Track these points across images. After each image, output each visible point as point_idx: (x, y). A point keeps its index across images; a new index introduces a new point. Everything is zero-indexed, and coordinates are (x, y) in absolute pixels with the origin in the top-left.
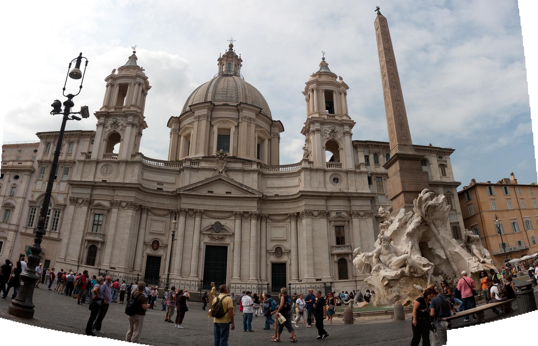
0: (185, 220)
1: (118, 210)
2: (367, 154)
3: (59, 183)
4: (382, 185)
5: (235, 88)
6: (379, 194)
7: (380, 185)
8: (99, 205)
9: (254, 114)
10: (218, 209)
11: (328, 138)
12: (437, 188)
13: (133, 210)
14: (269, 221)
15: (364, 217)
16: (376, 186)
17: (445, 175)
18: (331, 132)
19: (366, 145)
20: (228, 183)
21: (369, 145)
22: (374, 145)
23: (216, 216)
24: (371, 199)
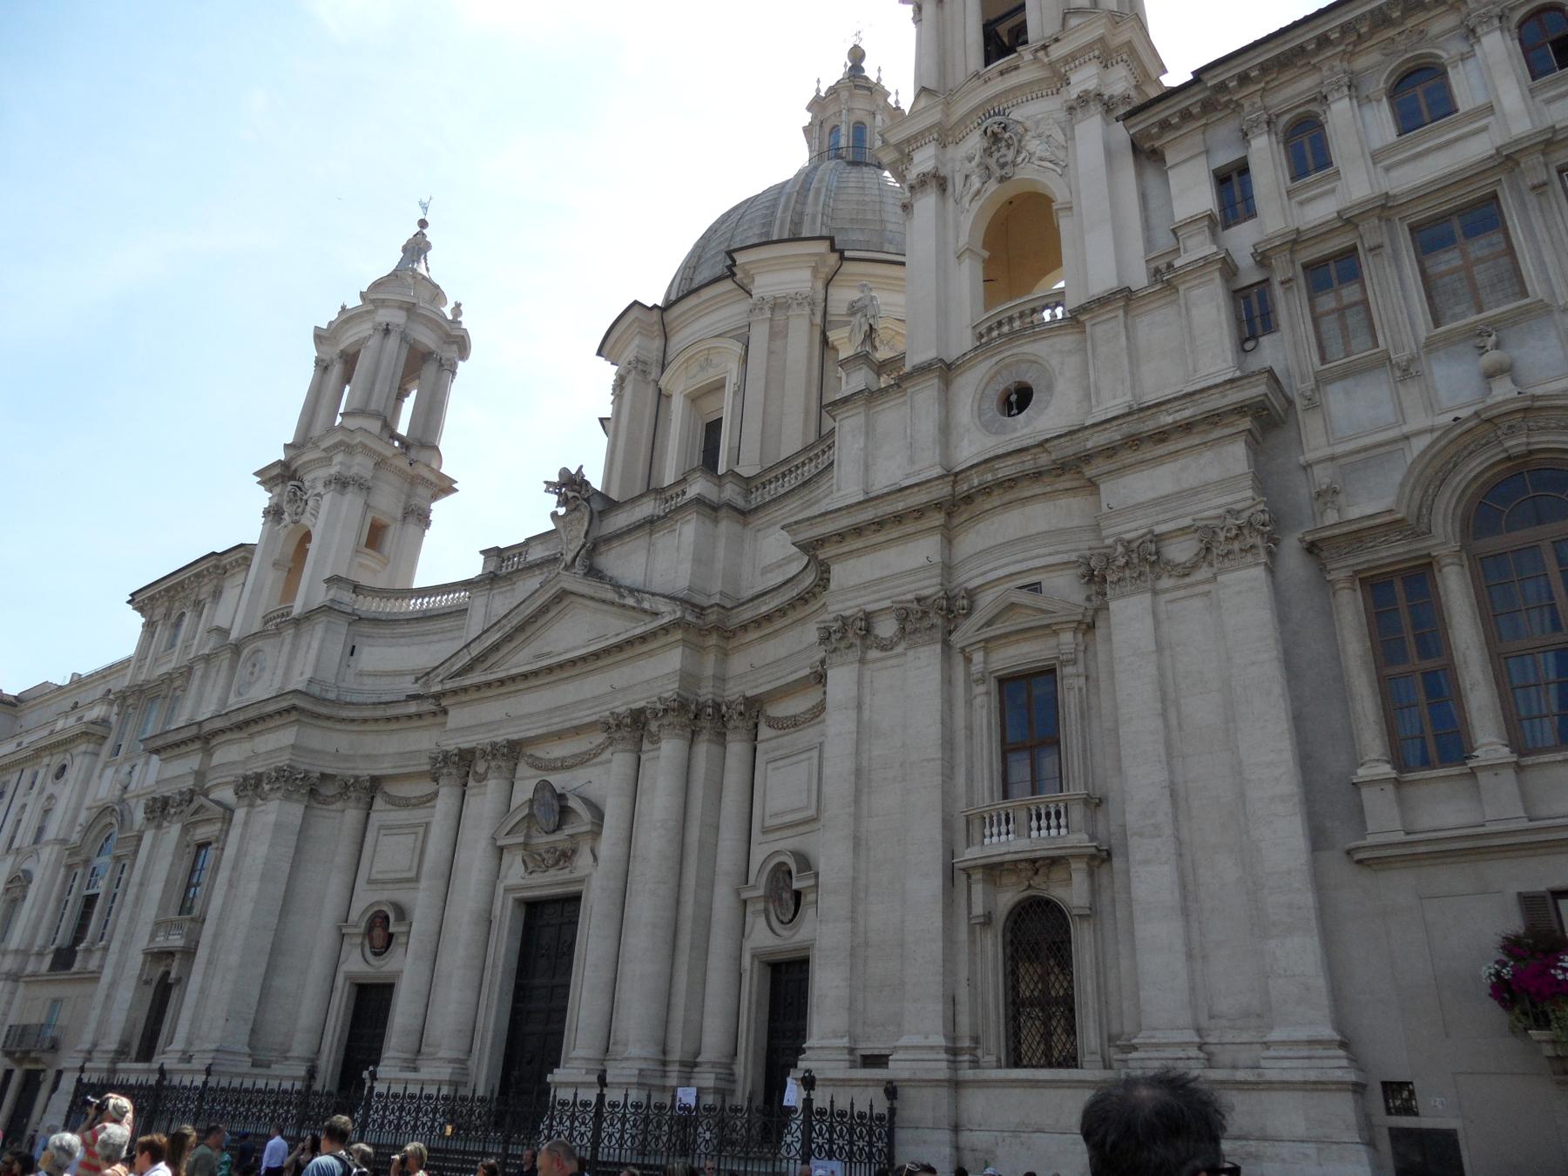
0: (458, 804)
1: (248, 813)
3: (147, 763)
4: (1365, 302)
5: (768, 208)
6: (1322, 381)
7: (1341, 311)
9: (807, 274)
10: (557, 723)
11: (978, 192)
13: (288, 797)
14: (765, 732)
15: (1203, 573)
18: (988, 152)
19: (1208, 106)
20: (592, 598)
21: (1222, 87)
22: (1264, 68)
23: (556, 759)
24: (1246, 423)
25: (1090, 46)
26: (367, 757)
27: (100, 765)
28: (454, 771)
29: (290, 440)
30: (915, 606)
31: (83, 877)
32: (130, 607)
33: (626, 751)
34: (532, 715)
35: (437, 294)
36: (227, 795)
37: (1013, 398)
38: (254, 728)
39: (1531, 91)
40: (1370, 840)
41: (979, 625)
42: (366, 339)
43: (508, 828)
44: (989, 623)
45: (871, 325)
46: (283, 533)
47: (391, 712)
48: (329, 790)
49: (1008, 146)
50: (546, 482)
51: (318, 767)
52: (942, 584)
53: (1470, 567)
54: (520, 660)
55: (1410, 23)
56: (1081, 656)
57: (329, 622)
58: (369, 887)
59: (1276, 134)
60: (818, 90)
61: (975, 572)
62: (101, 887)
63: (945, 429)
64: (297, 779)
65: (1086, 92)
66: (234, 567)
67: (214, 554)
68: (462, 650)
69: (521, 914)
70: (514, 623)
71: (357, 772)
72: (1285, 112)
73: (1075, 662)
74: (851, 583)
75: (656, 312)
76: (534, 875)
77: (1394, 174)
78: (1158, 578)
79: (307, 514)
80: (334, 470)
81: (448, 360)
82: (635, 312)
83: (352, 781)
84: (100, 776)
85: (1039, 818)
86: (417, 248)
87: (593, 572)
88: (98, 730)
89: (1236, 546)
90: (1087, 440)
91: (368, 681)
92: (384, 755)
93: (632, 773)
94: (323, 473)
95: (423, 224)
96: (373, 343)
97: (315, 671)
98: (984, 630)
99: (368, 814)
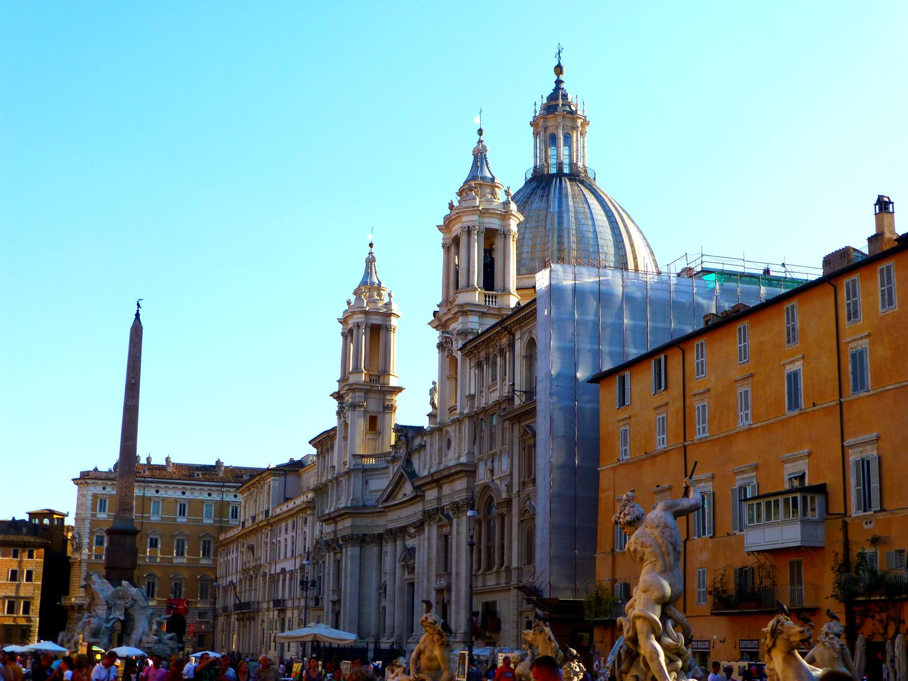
6: (480, 460)
8: (335, 549)
13: (353, 545)
29: (339, 377)
31: (318, 568)
38: (343, 517)
60: (535, 112)
62: (321, 575)
63: (440, 450)
77: (492, 394)
80: (350, 400)
86: (370, 262)
88: (310, 505)
91: (374, 494)
92: (381, 525)
95: (371, 245)
97: (353, 495)
99: (381, 548)
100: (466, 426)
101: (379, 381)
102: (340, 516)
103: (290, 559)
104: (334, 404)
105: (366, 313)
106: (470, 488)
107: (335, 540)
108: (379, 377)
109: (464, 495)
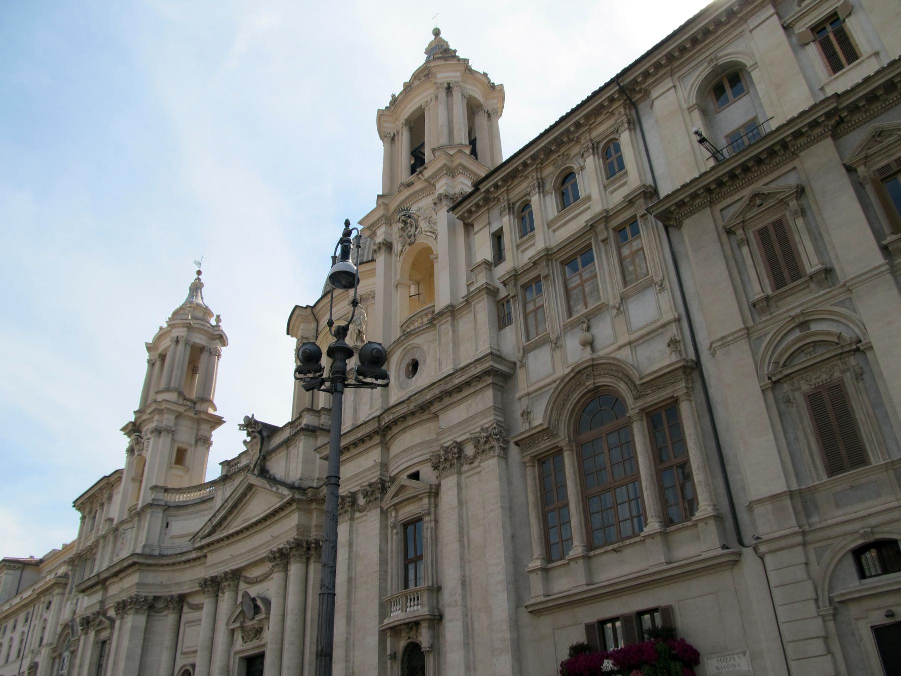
2: (495, 227)
6: (526, 351)
7: (535, 311)
12: (796, 163)
13: (137, 612)
16: (521, 322)
17: (852, 55)
18: (403, 229)
19: (486, 200)
22: (504, 180)
25: (441, 169)
26: (176, 584)
27: (65, 599)
28: (211, 589)
29: (137, 408)
30: (368, 488)
31: (59, 663)
32: (74, 509)
33: (279, 571)
34: (241, 555)
35: (207, 312)
36: (111, 613)
37: (411, 368)
38: (122, 575)
39: (605, 187)
40: (532, 602)
41: (391, 497)
42: (169, 346)
43: (232, 621)
44: (395, 496)
45: (359, 330)
46: (135, 461)
47: (184, 558)
48: (160, 605)
49: (412, 226)
50: (239, 425)
51: (151, 593)
52: (381, 474)
53: (577, 452)
54: (236, 525)
55: (562, 150)
56: (433, 510)
57: (152, 512)
58: (183, 656)
59: (513, 214)
61: (394, 467)
64: (140, 602)
65: (441, 194)
66: (116, 483)
67: (105, 477)
68: (208, 522)
69: (244, 665)
70: (230, 505)
71: (173, 593)
72: (517, 202)
73: (429, 514)
74: (348, 477)
75: (309, 310)
76: (247, 644)
77: (557, 233)
78: (462, 465)
79: (144, 451)
81: (214, 349)
82: (297, 312)
83: (169, 599)
84: (65, 607)
85: (411, 601)
86: (196, 288)
87: (264, 472)
89: (487, 446)
90: (427, 395)
91: (175, 541)
92: (185, 582)
93: (283, 583)
94: (151, 425)
95: (199, 273)
96: (173, 346)
98: (394, 499)
100: (483, 310)
101: (194, 408)
102: (116, 574)
103: (14, 662)
104: (125, 441)
105: (189, 328)
106: (502, 408)
107: (102, 612)
108: (194, 403)
109: (488, 420)
